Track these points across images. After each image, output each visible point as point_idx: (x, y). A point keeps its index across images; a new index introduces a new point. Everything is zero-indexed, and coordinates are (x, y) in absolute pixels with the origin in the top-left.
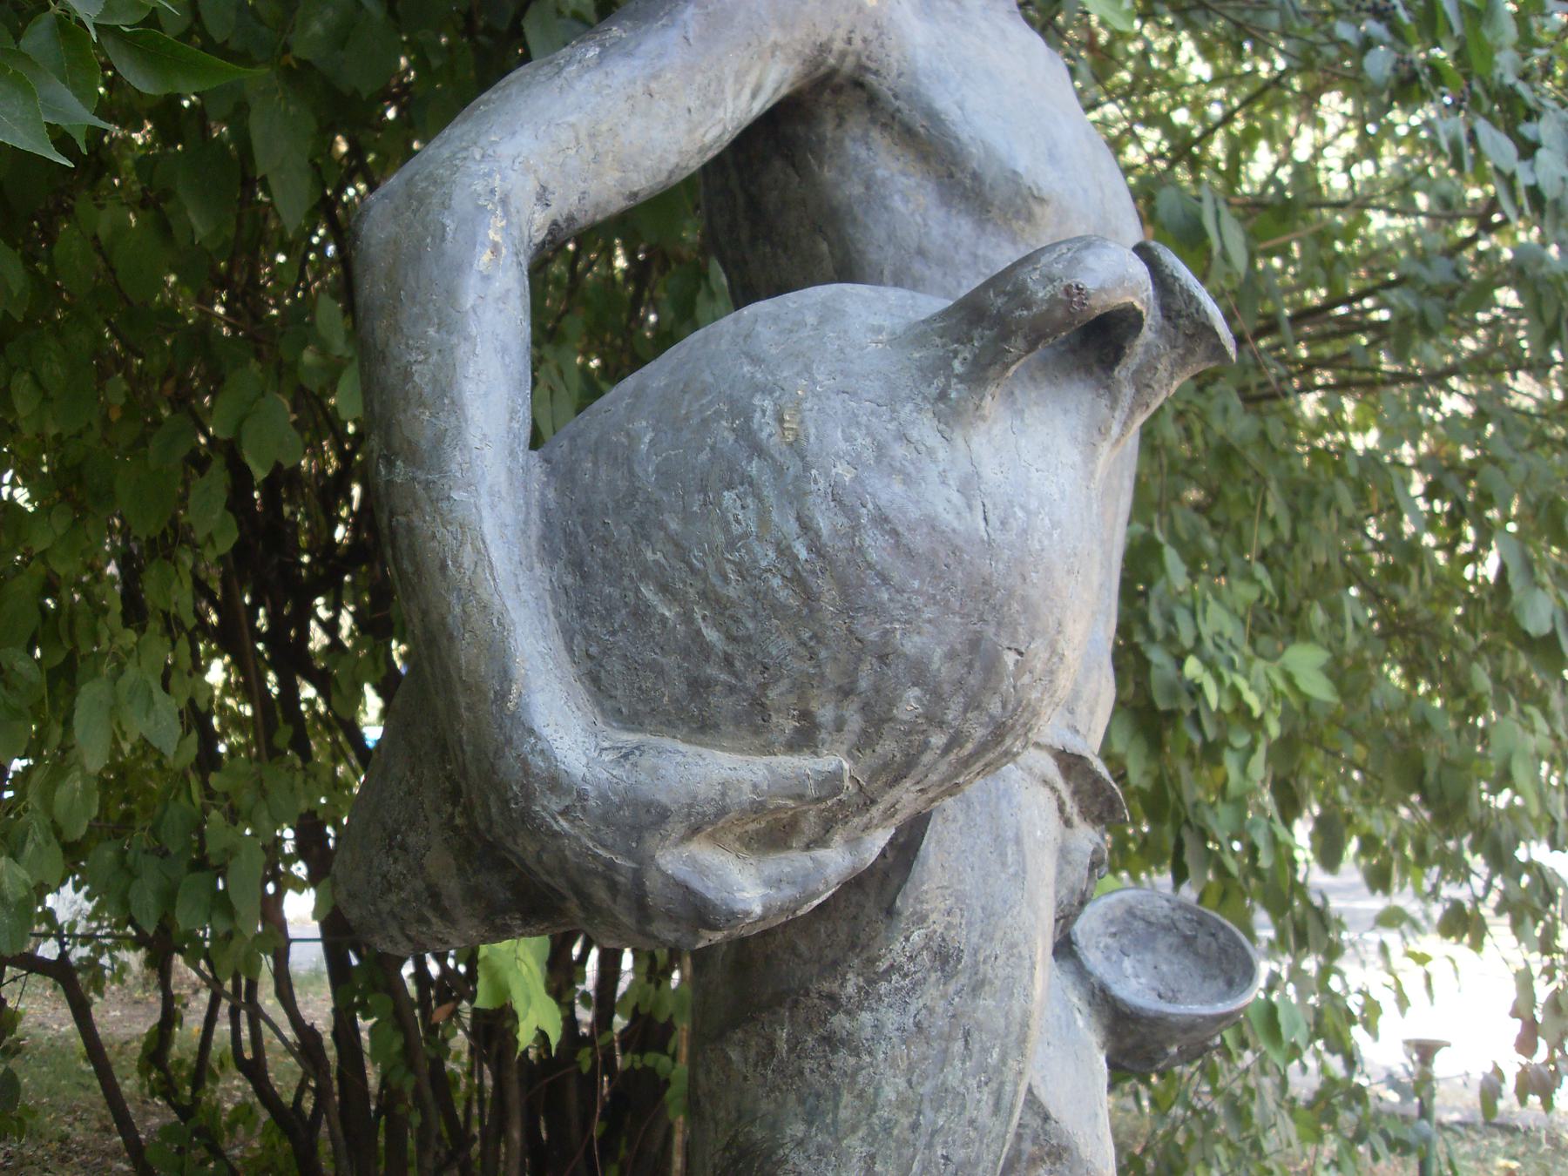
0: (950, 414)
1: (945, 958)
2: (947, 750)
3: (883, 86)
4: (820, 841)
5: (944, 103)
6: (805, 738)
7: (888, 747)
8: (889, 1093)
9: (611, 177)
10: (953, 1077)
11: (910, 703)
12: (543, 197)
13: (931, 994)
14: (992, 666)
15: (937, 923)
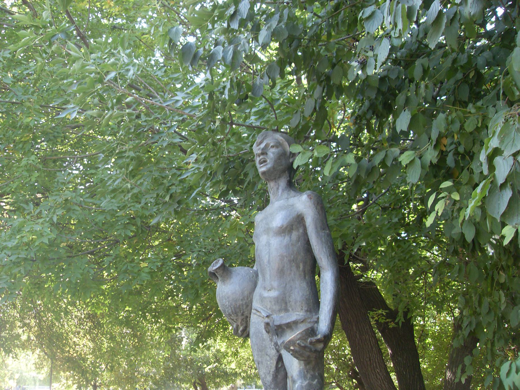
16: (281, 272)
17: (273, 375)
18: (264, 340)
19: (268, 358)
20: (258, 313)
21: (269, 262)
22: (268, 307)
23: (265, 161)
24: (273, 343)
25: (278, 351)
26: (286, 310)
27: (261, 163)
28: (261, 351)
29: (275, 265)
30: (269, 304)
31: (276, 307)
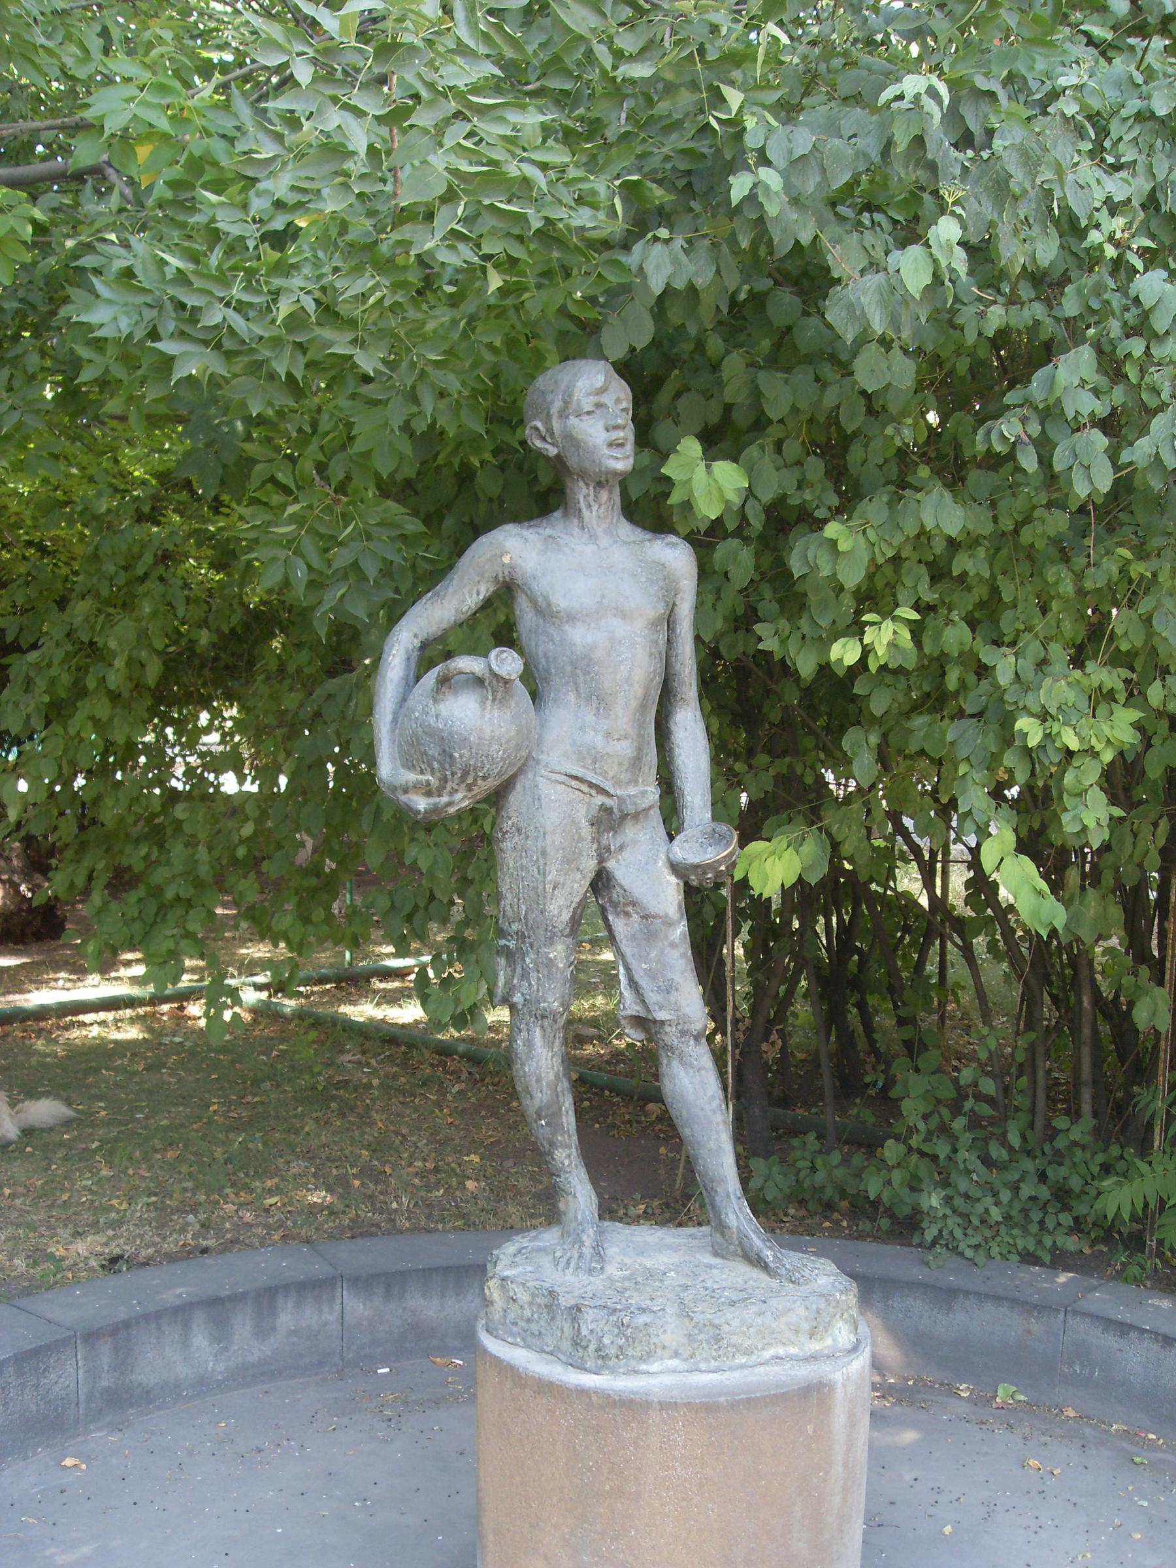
0: (435, 701)
1: (519, 830)
2: (453, 774)
3: (520, 582)
4: (440, 795)
5: (535, 587)
6: (422, 773)
7: (438, 774)
8: (511, 864)
9: (435, 628)
10: (524, 862)
11: (436, 765)
12: (416, 636)
13: (516, 839)
14: (451, 756)
15: (514, 819)
16: (643, 707)
17: (575, 909)
18: (581, 839)
19: (578, 876)
20: (573, 783)
21: (628, 680)
22: (611, 774)
23: (622, 445)
24: (595, 847)
25: (601, 860)
26: (636, 783)
27: (611, 445)
28: (569, 862)
29: (638, 691)
30: (616, 767)
31: (624, 777)
